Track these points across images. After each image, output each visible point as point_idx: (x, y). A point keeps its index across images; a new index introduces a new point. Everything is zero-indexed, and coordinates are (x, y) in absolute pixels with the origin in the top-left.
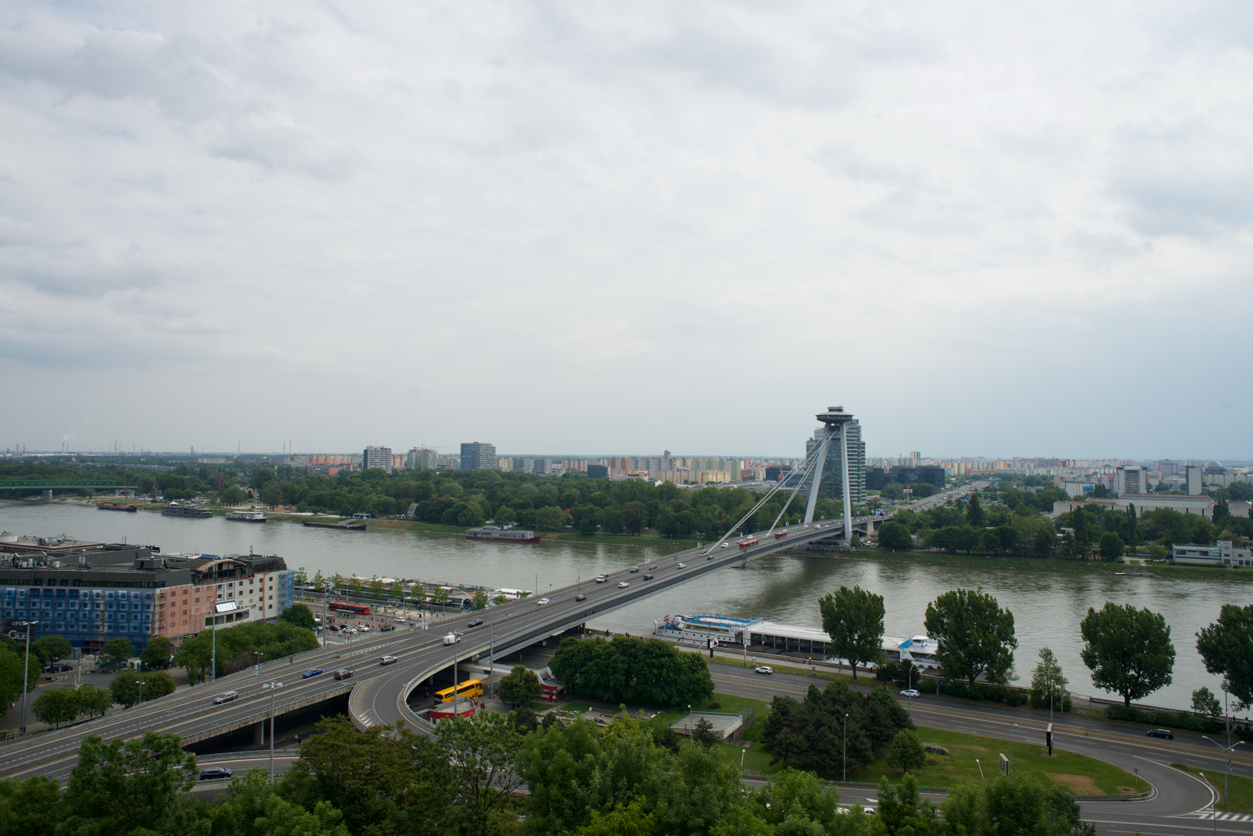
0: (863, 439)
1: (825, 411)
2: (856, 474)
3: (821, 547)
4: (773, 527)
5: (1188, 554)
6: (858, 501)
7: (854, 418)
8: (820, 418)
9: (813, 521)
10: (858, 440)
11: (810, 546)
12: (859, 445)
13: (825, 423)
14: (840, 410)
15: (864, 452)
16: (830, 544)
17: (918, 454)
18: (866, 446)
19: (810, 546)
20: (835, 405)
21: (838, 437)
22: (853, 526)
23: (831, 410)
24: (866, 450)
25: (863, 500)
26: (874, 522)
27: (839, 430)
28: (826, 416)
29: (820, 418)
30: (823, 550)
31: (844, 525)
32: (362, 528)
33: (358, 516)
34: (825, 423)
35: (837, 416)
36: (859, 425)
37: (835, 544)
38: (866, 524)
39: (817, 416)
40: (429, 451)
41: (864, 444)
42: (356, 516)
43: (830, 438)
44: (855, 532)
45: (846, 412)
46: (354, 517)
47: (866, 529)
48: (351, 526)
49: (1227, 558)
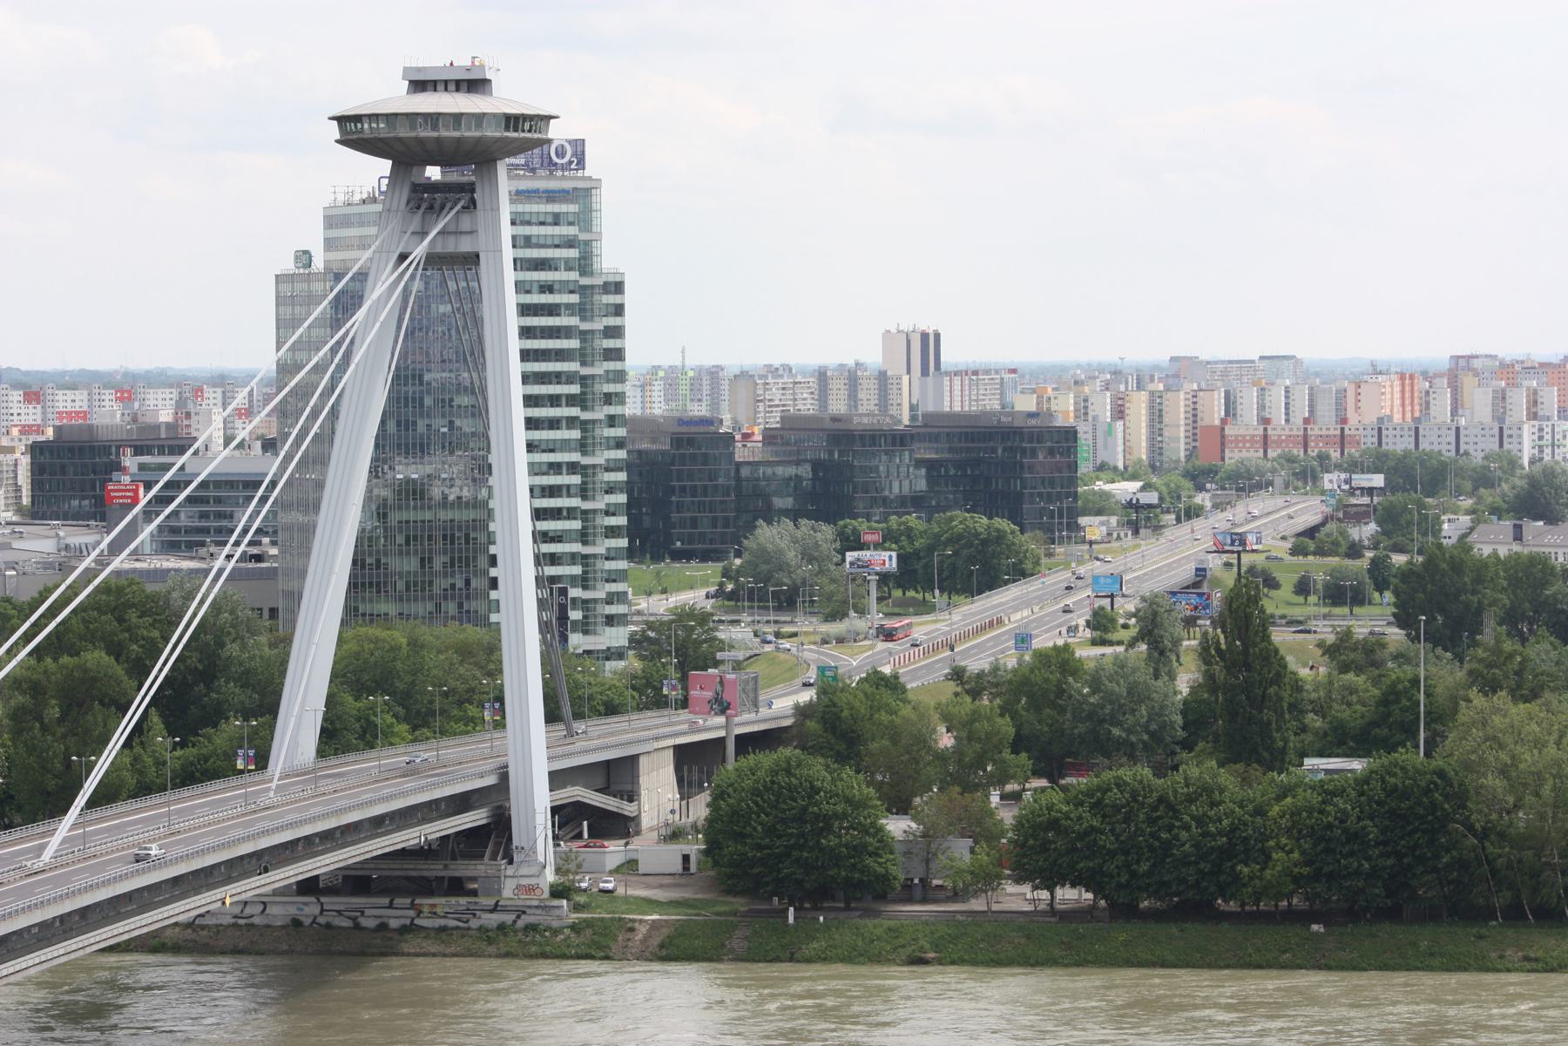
0: (610, 259)
1: (391, 96)
2: (573, 468)
3: (373, 910)
4: (81, 800)
7: (557, 132)
9: (321, 753)
11: (309, 908)
12: (584, 290)
13: (389, 163)
14: (476, 85)
15: (616, 332)
16: (428, 887)
17: (929, 344)
18: (630, 299)
19: (309, 908)
20: (436, 58)
21: (465, 245)
22: (558, 779)
23: (419, 86)
24: (631, 321)
25: (611, 620)
27: (472, 204)
28: (391, 118)
30: (383, 927)
31: (504, 777)
34: (384, 166)
35: (457, 118)
36: (590, 171)
37: (456, 887)
38: (634, 759)
39: (342, 120)
41: (618, 287)
43: (419, 251)
44: (567, 817)
45: (507, 97)
47: (632, 796)
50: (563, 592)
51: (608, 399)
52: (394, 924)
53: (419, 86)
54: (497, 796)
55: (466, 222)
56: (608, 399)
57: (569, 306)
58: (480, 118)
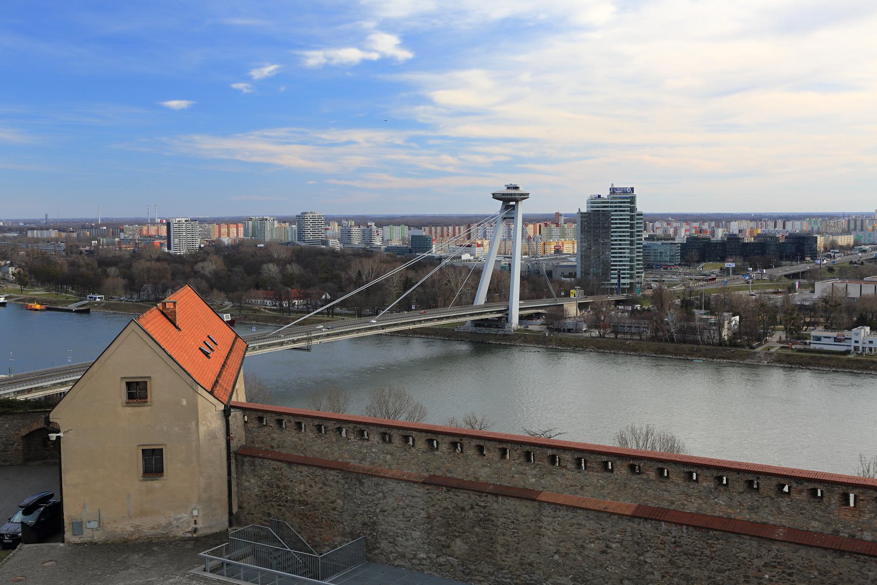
1: (504, 190)
5: (824, 341)
6: (631, 278)
8: (495, 196)
10: (633, 209)
13: (502, 202)
14: (516, 188)
22: (520, 309)
23: (508, 188)
26: (579, 303)
27: (514, 209)
29: (495, 196)
32: (87, 311)
33: (92, 297)
34: (502, 202)
40: (266, 219)
42: (90, 297)
45: (522, 190)
46: (88, 298)
48: (76, 309)
49: (856, 345)
50: (619, 272)
51: (638, 236)
52: (486, 332)
53: (508, 188)
54: (507, 312)
55: (513, 212)
56: (638, 236)
57: (628, 219)
58: (515, 194)
